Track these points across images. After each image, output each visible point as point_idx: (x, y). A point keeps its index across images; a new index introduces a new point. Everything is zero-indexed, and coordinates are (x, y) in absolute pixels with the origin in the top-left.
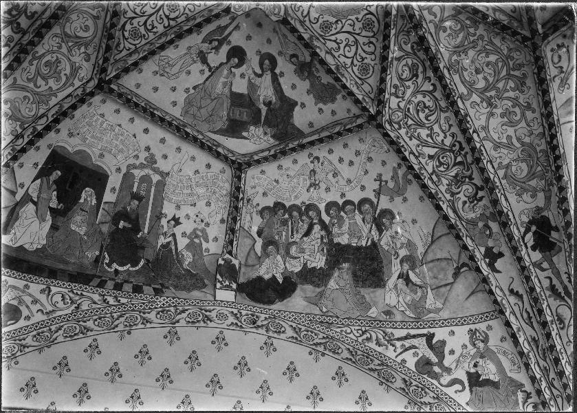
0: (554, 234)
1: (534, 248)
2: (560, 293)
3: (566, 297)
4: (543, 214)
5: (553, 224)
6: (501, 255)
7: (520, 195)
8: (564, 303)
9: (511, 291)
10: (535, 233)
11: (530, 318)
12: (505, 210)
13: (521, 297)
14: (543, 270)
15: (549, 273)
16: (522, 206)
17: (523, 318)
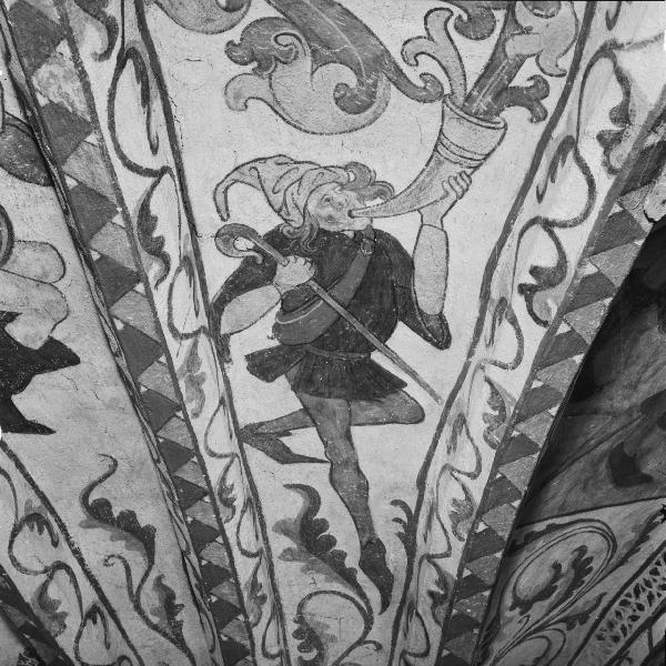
0: (404, 339)
1: (263, 366)
2: (343, 555)
3: (361, 577)
4: (379, 225)
5: (426, 299)
6: (57, 356)
7: (258, 58)
8: (351, 593)
9: (98, 513)
10: (291, 304)
11: (170, 606)
12: (133, 188)
13: (144, 538)
14: (286, 457)
15: (317, 476)
16: (261, 135)
17: (138, 607)
